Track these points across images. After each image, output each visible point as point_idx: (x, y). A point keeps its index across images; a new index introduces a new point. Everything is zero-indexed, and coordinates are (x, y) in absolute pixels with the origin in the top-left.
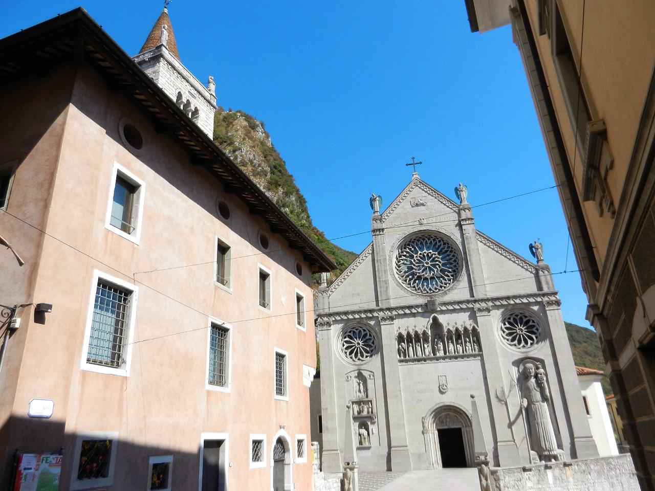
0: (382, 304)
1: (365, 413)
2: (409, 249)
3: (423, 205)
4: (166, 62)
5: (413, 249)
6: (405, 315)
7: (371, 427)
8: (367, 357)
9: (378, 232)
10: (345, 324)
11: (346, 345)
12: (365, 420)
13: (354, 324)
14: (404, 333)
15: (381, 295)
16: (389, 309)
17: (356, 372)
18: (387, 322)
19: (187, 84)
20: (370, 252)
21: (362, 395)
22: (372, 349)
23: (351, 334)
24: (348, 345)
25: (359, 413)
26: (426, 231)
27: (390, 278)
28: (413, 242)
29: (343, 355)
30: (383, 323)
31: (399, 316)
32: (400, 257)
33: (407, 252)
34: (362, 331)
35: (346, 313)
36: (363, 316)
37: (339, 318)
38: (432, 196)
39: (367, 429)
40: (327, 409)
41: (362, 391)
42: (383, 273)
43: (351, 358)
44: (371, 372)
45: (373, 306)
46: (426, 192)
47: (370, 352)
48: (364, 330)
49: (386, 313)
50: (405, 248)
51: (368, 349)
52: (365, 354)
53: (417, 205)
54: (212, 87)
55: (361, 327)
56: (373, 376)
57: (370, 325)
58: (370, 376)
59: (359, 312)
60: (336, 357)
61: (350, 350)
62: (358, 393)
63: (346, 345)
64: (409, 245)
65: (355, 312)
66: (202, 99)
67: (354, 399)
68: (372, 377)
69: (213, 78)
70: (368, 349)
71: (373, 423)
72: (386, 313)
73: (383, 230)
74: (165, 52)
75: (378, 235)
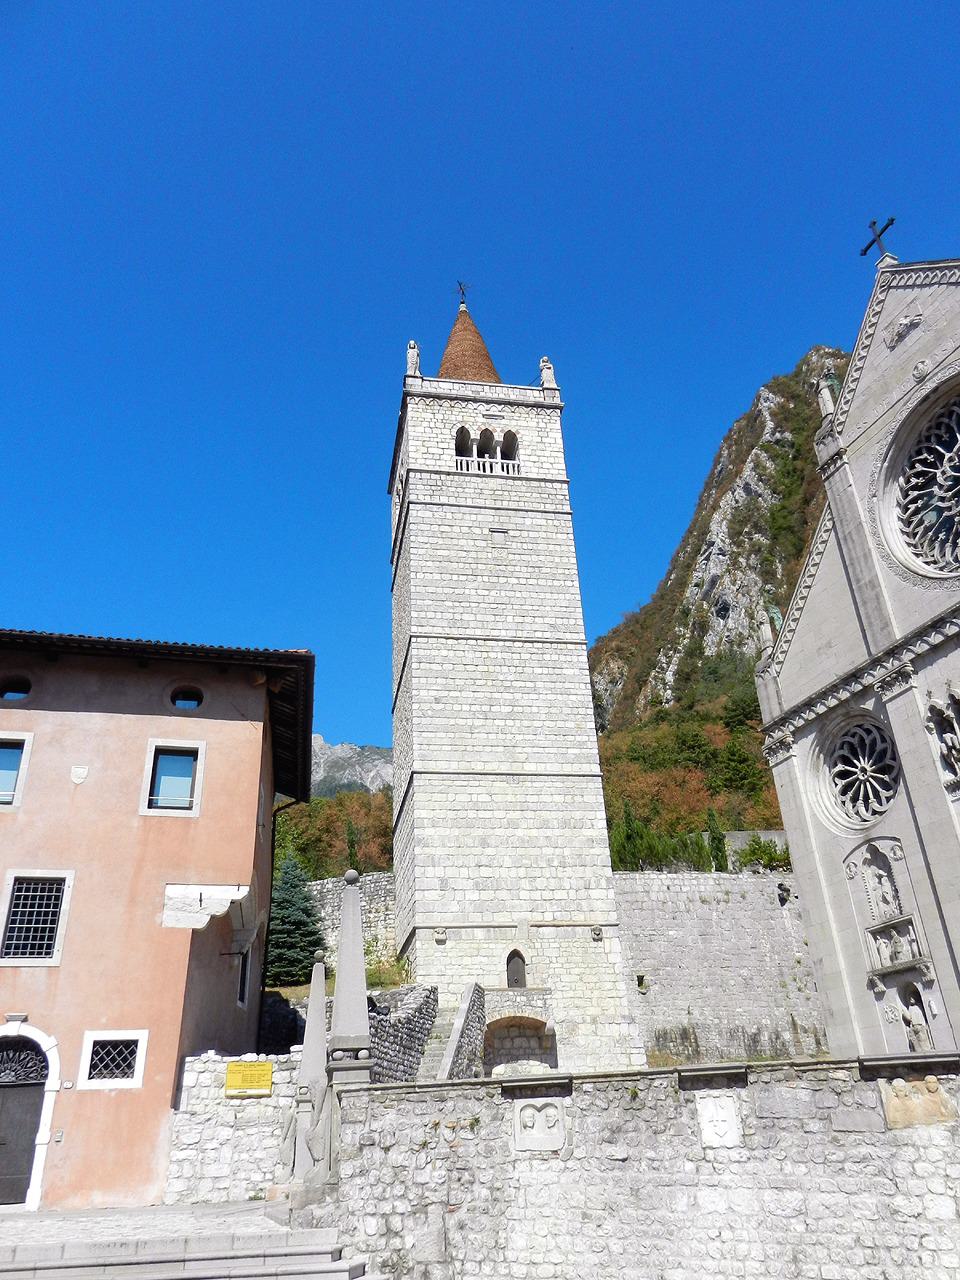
0: (876, 645)
1: (905, 958)
2: (920, 461)
3: (913, 326)
4: (417, 399)
5: (931, 458)
6: (936, 651)
7: (925, 996)
8: (888, 799)
9: (832, 468)
10: (821, 731)
11: (841, 783)
12: (908, 977)
13: (832, 726)
14: (941, 702)
15: (870, 624)
16: (893, 652)
17: (864, 848)
18: (897, 690)
19: (475, 405)
20: (829, 525)
21: (883, 913)
22: (893, 775)
23: (845, 752)
24: (844, 782)
25: (894, 956)
26: (942, 389)
27: (879, 568)
28: (928, 439)
29: (839, 814)
30: (889, 695)
31: (920, 661)
32: (906, 496)
33: (918, 475)
34: (864, 735)
35: (809, 704)
36: (844, 695)
37: (802, 722)
38: (930, 285)
39: (919, 1002)
40: (821, 960)
41: (889, 898)
42: (863, 564)
43: (857, 813)
44: (895, 839)
45: (861, 658)
46: (912, 286)
47: (892, 783)
48: (869, 732)
49: (889, 665)
50: (912, 467)
51: (886, 778)
52: (884, 794)
53: (901, 337)
54: (548, 376)
55: (860, 726)
56: (902, 849)
57: (865, 714)
58: (895, 854)
59: (833, 689)
60: (818, 824)
61: (850, 794)
62: (881, 904)
63: (841, 783)
64: (919, 453)
65: (835, 686)
66: (523, 410)
67: (874, 923)
68: (899, 853)
69: (545, 358)
70: (886, 778)
71: (929, 984)
72: (889, 665)
73: (839, 454)
74: (415, 385)
75: (833, 474)
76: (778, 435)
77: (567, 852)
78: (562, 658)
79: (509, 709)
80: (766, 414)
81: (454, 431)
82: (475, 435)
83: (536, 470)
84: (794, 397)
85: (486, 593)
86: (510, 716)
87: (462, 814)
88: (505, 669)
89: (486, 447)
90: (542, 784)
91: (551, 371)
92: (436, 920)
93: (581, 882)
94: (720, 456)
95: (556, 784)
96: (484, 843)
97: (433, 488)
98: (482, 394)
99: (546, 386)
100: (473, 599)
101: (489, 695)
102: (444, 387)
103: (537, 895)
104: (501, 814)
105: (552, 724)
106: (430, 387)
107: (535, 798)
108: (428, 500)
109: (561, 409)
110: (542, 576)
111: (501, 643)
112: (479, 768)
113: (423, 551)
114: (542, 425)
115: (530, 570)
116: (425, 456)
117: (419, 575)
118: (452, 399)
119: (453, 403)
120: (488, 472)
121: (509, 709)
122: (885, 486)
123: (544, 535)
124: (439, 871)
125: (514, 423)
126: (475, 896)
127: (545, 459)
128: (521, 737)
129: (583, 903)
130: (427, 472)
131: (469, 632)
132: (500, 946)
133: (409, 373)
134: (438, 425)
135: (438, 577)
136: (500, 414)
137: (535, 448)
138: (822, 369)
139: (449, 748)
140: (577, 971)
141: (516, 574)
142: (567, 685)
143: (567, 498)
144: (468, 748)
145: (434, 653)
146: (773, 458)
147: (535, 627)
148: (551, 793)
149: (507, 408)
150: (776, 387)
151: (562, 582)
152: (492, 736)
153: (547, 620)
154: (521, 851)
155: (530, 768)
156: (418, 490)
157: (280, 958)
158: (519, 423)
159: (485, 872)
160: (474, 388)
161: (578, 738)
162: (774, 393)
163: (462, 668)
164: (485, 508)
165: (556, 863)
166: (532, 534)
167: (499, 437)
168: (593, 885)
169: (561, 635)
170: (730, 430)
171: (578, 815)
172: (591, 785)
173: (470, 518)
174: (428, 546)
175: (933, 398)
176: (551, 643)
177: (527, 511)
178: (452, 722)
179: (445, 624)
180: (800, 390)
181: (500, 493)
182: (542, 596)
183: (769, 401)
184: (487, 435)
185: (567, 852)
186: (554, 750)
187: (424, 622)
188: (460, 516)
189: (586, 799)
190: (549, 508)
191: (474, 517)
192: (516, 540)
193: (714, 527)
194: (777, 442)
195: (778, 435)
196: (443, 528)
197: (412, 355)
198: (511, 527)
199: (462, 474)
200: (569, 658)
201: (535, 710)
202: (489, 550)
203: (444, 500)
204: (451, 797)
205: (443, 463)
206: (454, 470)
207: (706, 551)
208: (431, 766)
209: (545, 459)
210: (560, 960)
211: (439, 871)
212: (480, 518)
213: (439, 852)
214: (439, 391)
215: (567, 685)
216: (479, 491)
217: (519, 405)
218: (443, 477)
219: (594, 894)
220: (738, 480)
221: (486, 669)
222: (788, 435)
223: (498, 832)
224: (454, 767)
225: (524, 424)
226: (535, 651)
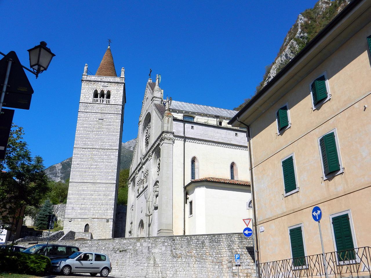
31: (139, 171)
76: (302, 34)
77: (104, 202)
78: (112, 153)
79: (95, 166)
80: (299, 25)
82: (99, 92)
84: (311, 18)
85: (95, 136)
86: (95, 168)
87: (80, 192)
88: (96, 156)
89: (102, 95)
90: (100, 185)
91: (124, 72)
92: (70, 216)
93: (106, 209)
94: (286, 39)
95: (104, 185)
96: (84, 199)
98: (103, 80)
99: (121, 77)
100: (91, 138)
102: (93, 78)
103: (94, 212)
104: (89, 192)
105: (106, 170)
106: (89, 78)
107: (98, 189)
108: (83, 111)
109: (124, 84)
111: (96, 150)
112: (86, 181)
114: (118, 88)
117: (78, 132)
118: (94, 81)
119: (95, 82)
120: (101, 103)
121: (95, 166)
122: (143, 131)
123: (113, 120)
124: (72, 205)
125: (110, 88)
126: (80, 211)
128: (97, 174)
129: (105, 213)
130: (84, 103)
132: (84, 223)
133: (84, 74)
135: (83, 132)
136: (107, 85)
137: (115, 95)
138: (322, 8)
139: (79, 176)
140: (101, 229)
141: (103, 131)
143: (121, 110)
144: (84, 176)
145: (79, 152)
146: (298, 44)
147: (106, 145)
148: (103, 188)
149: (109, 84)
150: (307, 15)
152: (90, 173)
153: (109, 143)
154: (92, 201)
155: (98, 181)
156: (81, 108)
157: (41, 223)
159: (83, 206)
160: (101, 78)
161: (112, 174)
162: (304, 17)
165: (101, 204)
166: (110, 120)
167: (105, 92)
168: (109, 210)
169: (112, 147)
170: (291, 29)
171: (108, 193)
173: (95, 115)
174: (82, 124)
177: (109, 114)
178: (81, 170)
180: (314, 16)
181: (103, 108)
182: (109, 137)
183: (302, 20)
184: (102, 92)
185: (104, 202)
186: (105, 177)
187: (77, 144)
188: (91, 115)
190: (116, 112)
191: (95, 115)
192: (105, 122)
193: (271, 71)
194: (301, 37)
195: (302, 34)
196: (86, 119)
197: (86, 68)
198: (104, 118)
199: (94, 103)
201: (102, 167)
202: (98, 124)
203: (88, 111)
204: (78, 188)
206: (92, 102)
207: (268, 80)
208: (74, 181)
210: (98, 226)
211: (72, 205)
213: (73, 201)
214: (92, 79)
215: (111, 161)
216: (98, 108)
217: (112, 83)
219: (108, 211)
220: (283, 52)
222: (306, 34)
223: (88, 196)
224: (79, 181)
225: (113, 88)
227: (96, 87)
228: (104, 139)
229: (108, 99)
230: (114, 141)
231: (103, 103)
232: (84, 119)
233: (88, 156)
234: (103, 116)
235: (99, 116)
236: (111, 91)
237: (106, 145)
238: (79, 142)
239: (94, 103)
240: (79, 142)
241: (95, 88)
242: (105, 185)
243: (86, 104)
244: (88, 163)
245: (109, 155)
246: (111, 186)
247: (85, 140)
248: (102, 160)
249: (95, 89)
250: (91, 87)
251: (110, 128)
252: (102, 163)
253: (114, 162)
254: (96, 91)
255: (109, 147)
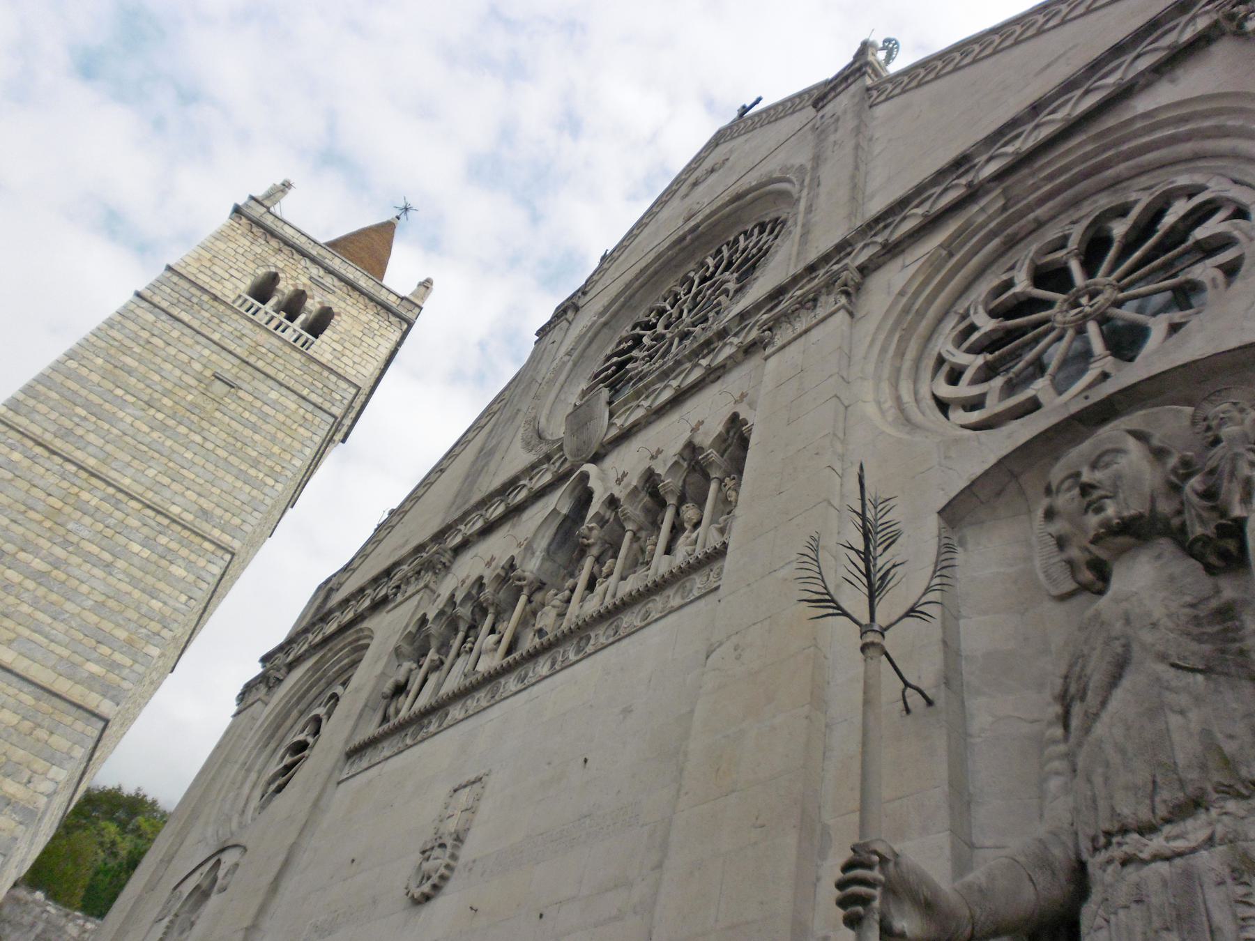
78: (184, 552)
81: (261, 272)
82: (285, 287)
83: (330, 357)
85: (146, 429)
86: (39, 577)
88: (87, 520)
97: (182, 299)
101: (31, 536)
108: (164, 305)
110: (239, 454)
111: (111, 490)
113: (103, 345)
115: (231, 440)
116: (202, 269)
123: (281, 417)
125: (343, 305)
127: (350, 355)
131: (79, 455)
134: (247, 254)
135: (95, 378)
137: (347, 339)
141: (206, 434)
142: (161, 585)
147: (178, 499)
151: (261, 475)
153: (202, 501)
158: (349, 308)
163: (25, 485)
164: (230, 352)
167: (313, 305)
172: (79, 725)
175: (689, 238)
176: (185, 527)
179: (53, 428)
188: (189, 341)
189: (55, 740)
192: (239, 402)
198: (245, 386)
200: (193, 557)
203: (185, 317)
205: (219, 287)
209: (350, 355)
212: (214, 357)
215: (161, 585)
218: (205, 298)
221: (59, 504)
225: (354, 312)
226: (153, 524)
227: (281, 265)
228: (186, 465)
229: (307, 335)
230: (238, 503)
231: (278, 332)
232: (145, 335)
233: (42, 495)
234: (242, 374)
235: (228, 366)
236: (339, 314)
237: (178, 499)
238: (42, 408)
239: (237, 312)
240: (40, 407)
241: (276, 267)
242: (28, 699)
243: (193, 290)
244: (14, 527)
245: (167, 555)
246: (69, 720)
247: (79, 416)
248: (107, 556)
249: (273, 270)
250: (259, 251)
251: (248, 441)
252: (96, 571)
253: (171, 602)
254: (273, 279)
255: (189, 517)
